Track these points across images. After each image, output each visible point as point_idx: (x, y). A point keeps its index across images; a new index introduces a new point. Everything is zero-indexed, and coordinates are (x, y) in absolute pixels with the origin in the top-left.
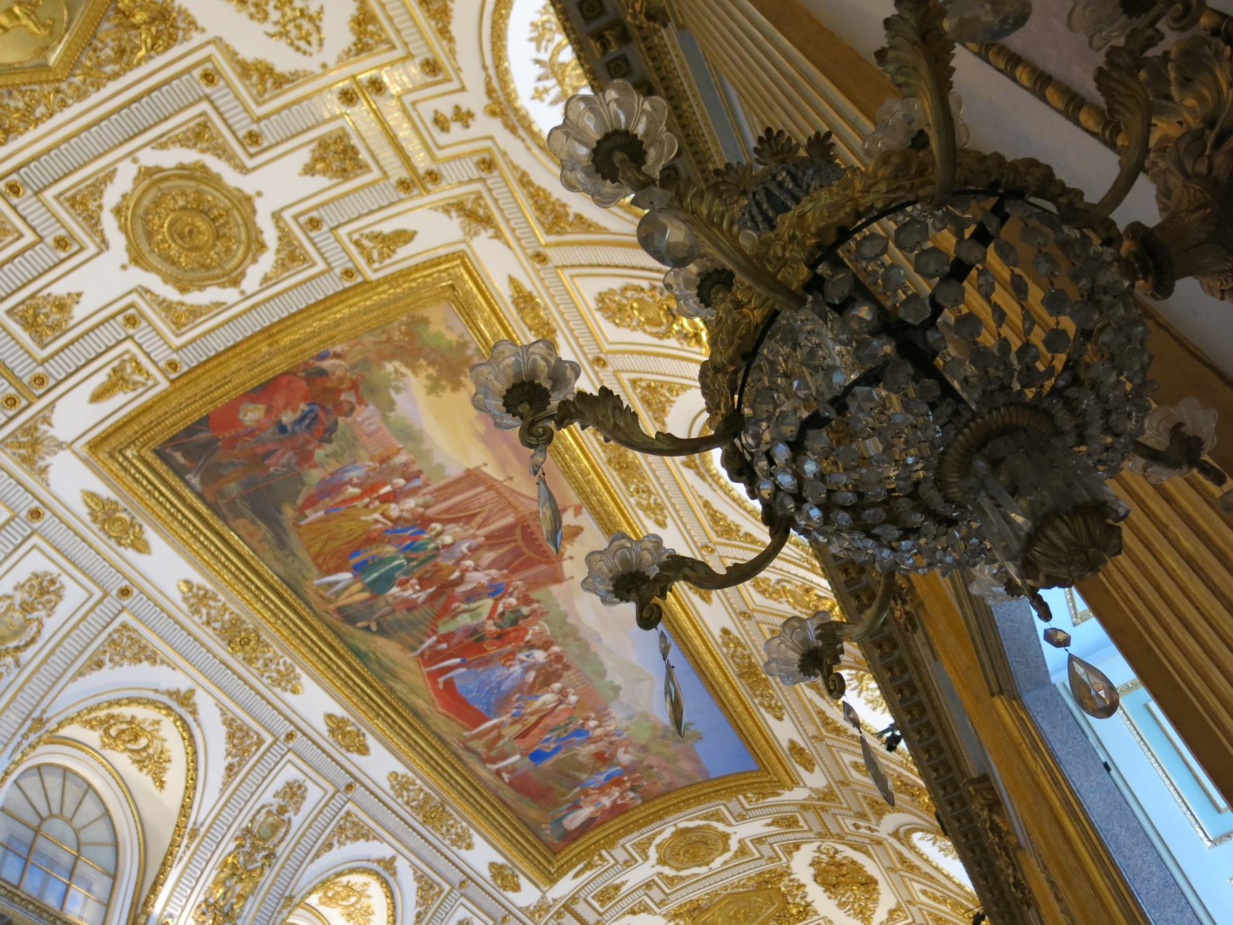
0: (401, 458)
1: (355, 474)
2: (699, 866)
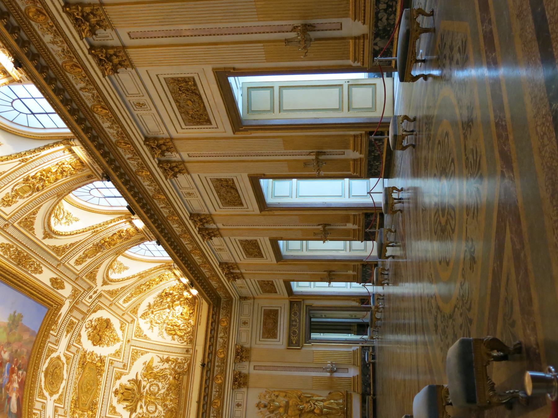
2: (62, 383)
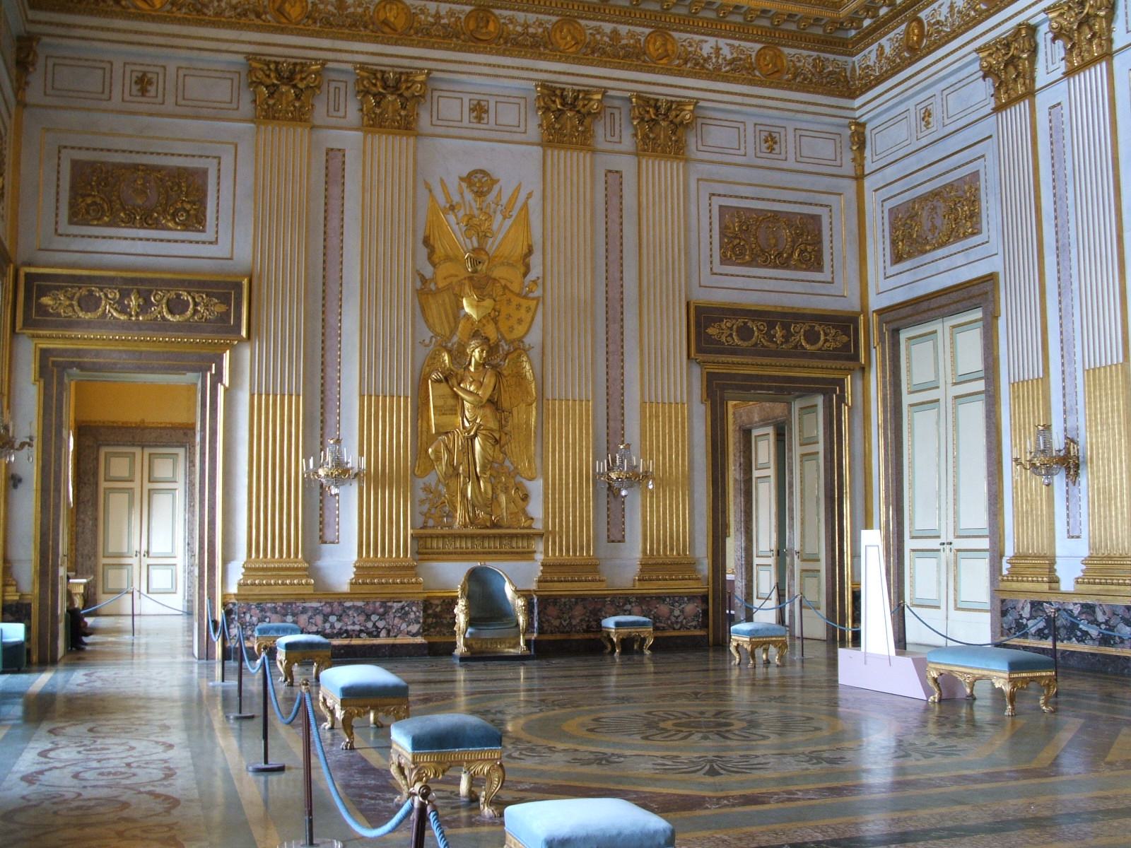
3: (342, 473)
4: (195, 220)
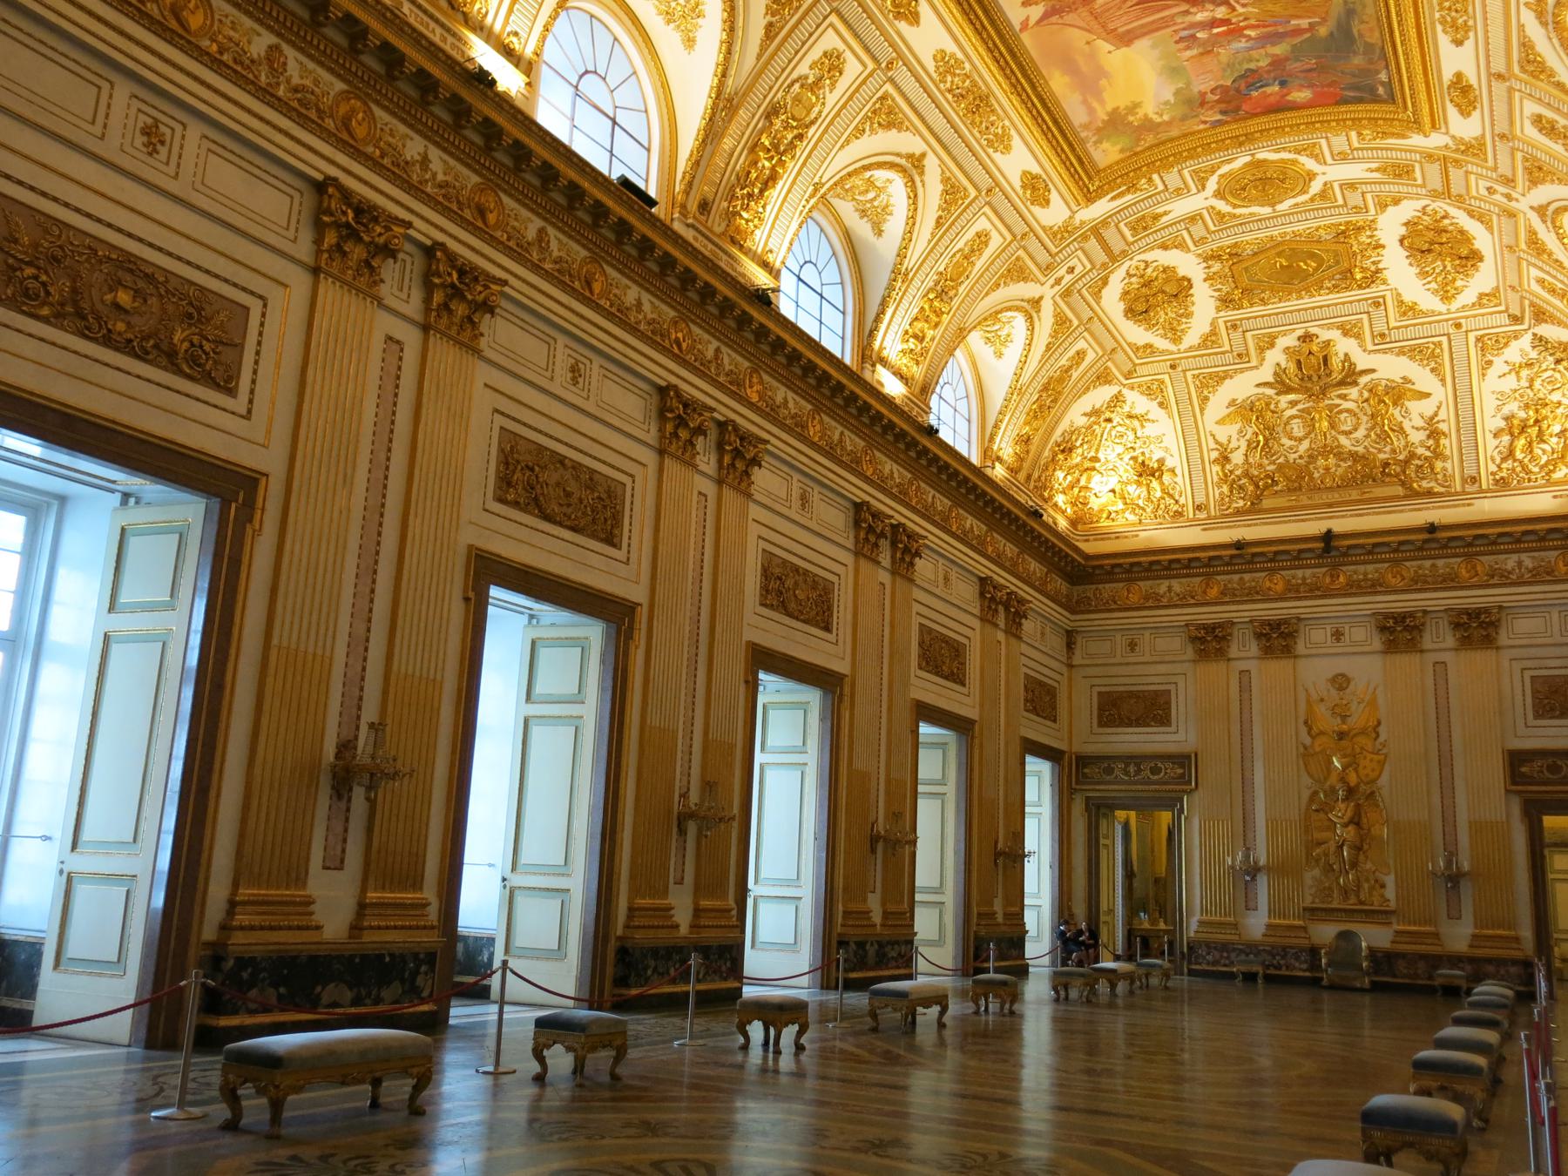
0: (1189, 53)
1: (1243, 44)
3: (1254, 871)
4: (1164, 720)
